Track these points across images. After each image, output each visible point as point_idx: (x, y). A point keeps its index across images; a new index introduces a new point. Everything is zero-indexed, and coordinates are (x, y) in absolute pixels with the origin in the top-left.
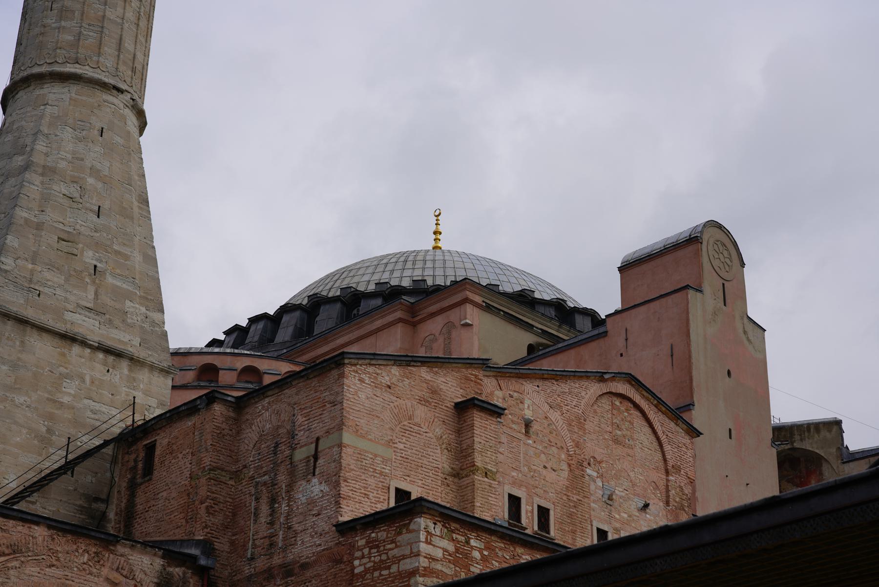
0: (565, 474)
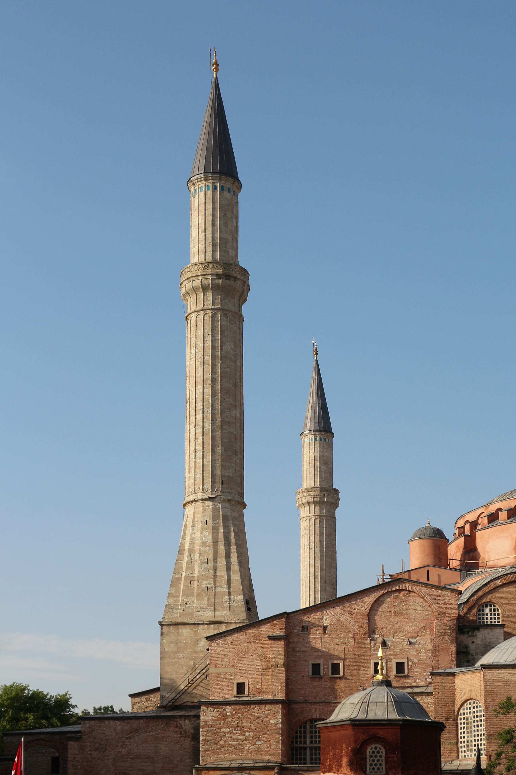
0: (353, 643)
